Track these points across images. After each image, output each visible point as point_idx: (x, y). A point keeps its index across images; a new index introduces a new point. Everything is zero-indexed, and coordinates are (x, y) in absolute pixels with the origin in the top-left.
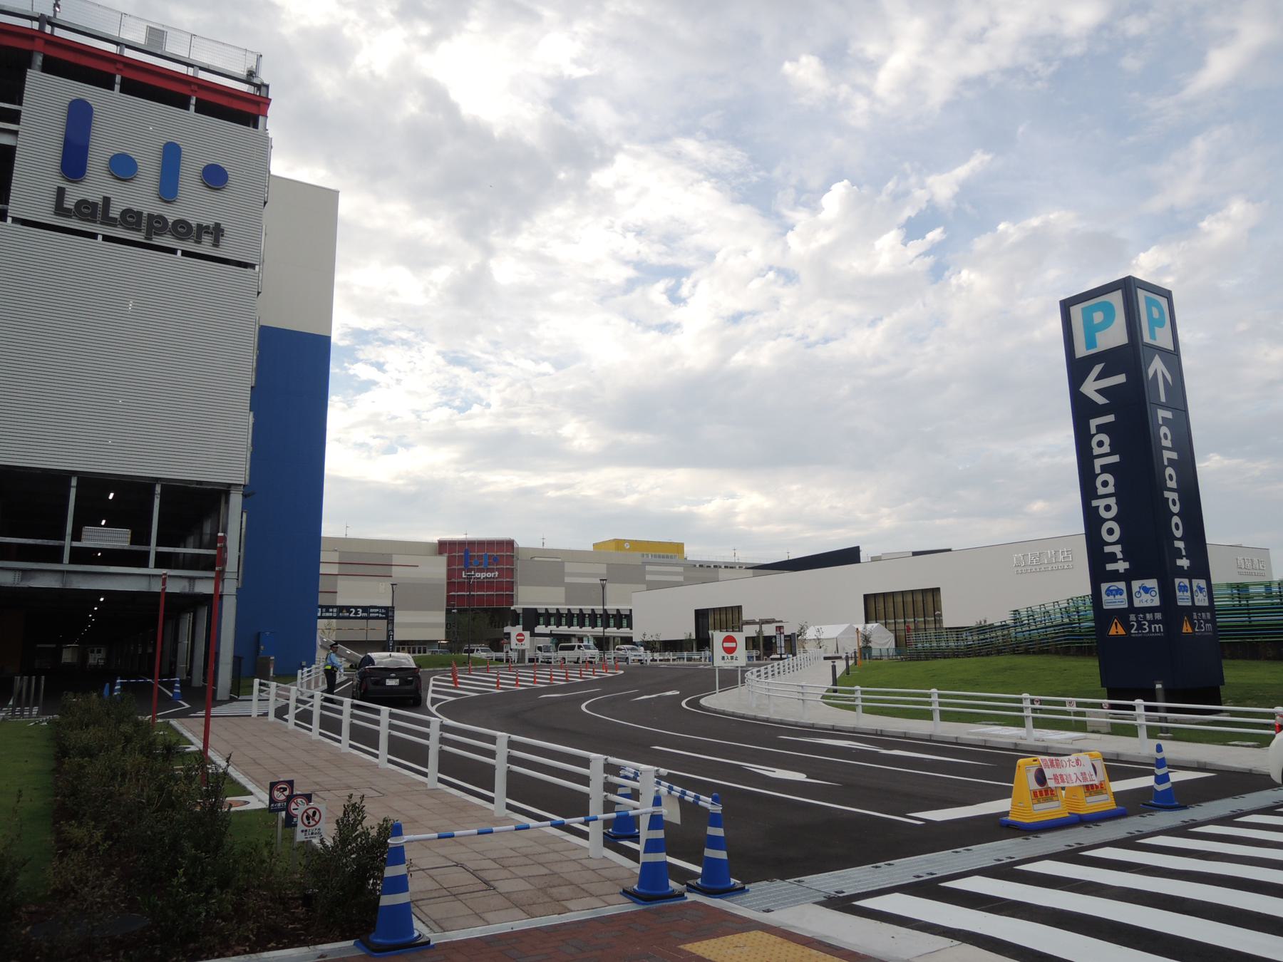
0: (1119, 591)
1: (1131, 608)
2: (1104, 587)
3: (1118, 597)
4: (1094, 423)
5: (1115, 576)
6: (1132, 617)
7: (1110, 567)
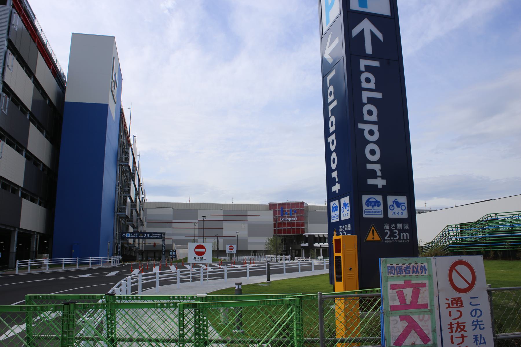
0: (377, 203)
1: (386, 219)
2: (365, 198)
3: (376, 208)
4: (363, 63)
5: (374, 190)
6: (387, 226)
7: (370, 182)
